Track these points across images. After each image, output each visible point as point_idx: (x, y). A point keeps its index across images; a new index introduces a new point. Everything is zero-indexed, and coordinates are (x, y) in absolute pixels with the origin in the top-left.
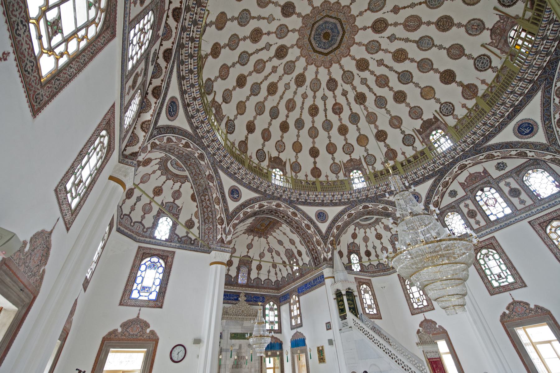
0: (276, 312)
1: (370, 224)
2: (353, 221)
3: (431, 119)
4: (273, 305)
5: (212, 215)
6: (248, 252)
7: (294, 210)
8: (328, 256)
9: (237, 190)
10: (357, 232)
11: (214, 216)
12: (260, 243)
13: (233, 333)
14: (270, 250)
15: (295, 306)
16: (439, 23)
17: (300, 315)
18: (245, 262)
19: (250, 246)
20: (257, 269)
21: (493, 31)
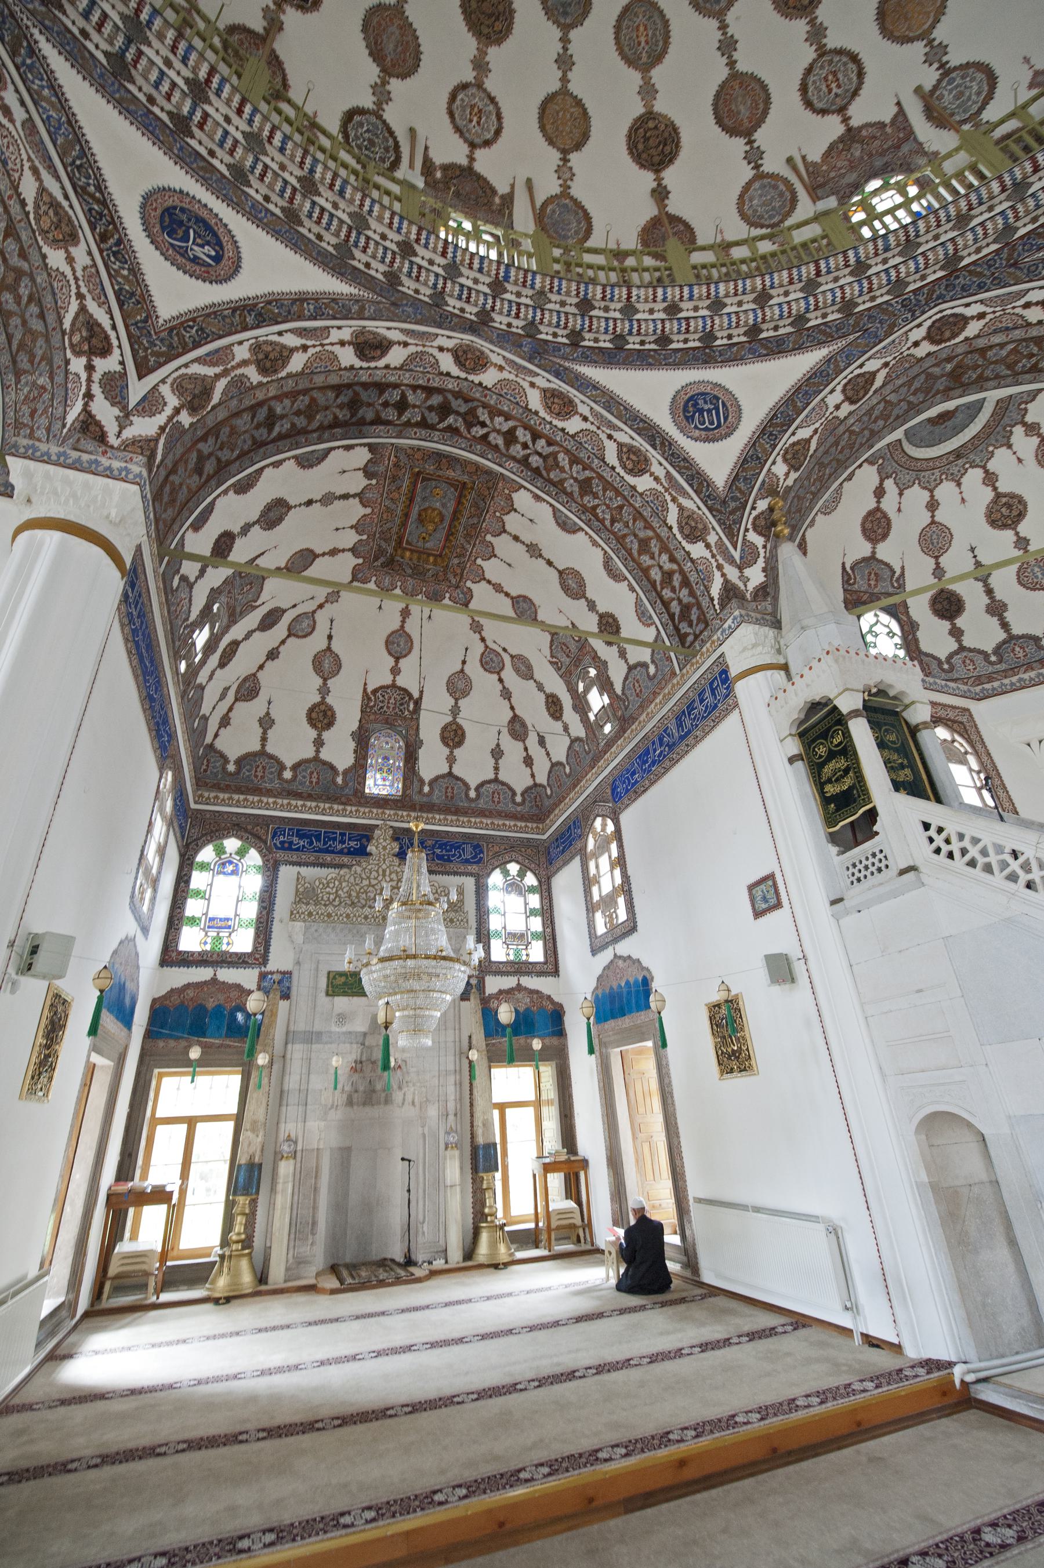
0: (534, 901)
1: (958, 454)
2: (875, 435)
4: (522, 874)
5: (42, 316)
6: (395, 671)
7: (557, 384)
8: (746, 581)
9: (200, 221)
10: (889, 504)
11: (51, 318)
12: (442, 635)
13: (342, 974)
14: (491, 662)
15: (604, 861)
17: (626, 888)
18: (391, 711)
19: (398, 645)
20: (444, 739)
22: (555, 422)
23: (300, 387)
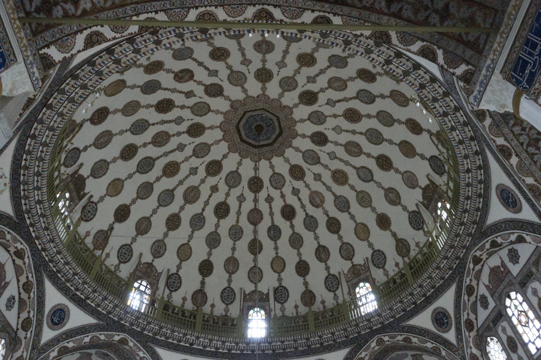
3: (84, 189)
16: (176, 217)
21: (150, 265)
22: (203, 9)
23: (367, 12)
